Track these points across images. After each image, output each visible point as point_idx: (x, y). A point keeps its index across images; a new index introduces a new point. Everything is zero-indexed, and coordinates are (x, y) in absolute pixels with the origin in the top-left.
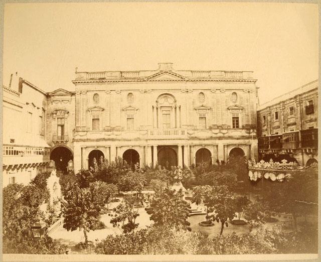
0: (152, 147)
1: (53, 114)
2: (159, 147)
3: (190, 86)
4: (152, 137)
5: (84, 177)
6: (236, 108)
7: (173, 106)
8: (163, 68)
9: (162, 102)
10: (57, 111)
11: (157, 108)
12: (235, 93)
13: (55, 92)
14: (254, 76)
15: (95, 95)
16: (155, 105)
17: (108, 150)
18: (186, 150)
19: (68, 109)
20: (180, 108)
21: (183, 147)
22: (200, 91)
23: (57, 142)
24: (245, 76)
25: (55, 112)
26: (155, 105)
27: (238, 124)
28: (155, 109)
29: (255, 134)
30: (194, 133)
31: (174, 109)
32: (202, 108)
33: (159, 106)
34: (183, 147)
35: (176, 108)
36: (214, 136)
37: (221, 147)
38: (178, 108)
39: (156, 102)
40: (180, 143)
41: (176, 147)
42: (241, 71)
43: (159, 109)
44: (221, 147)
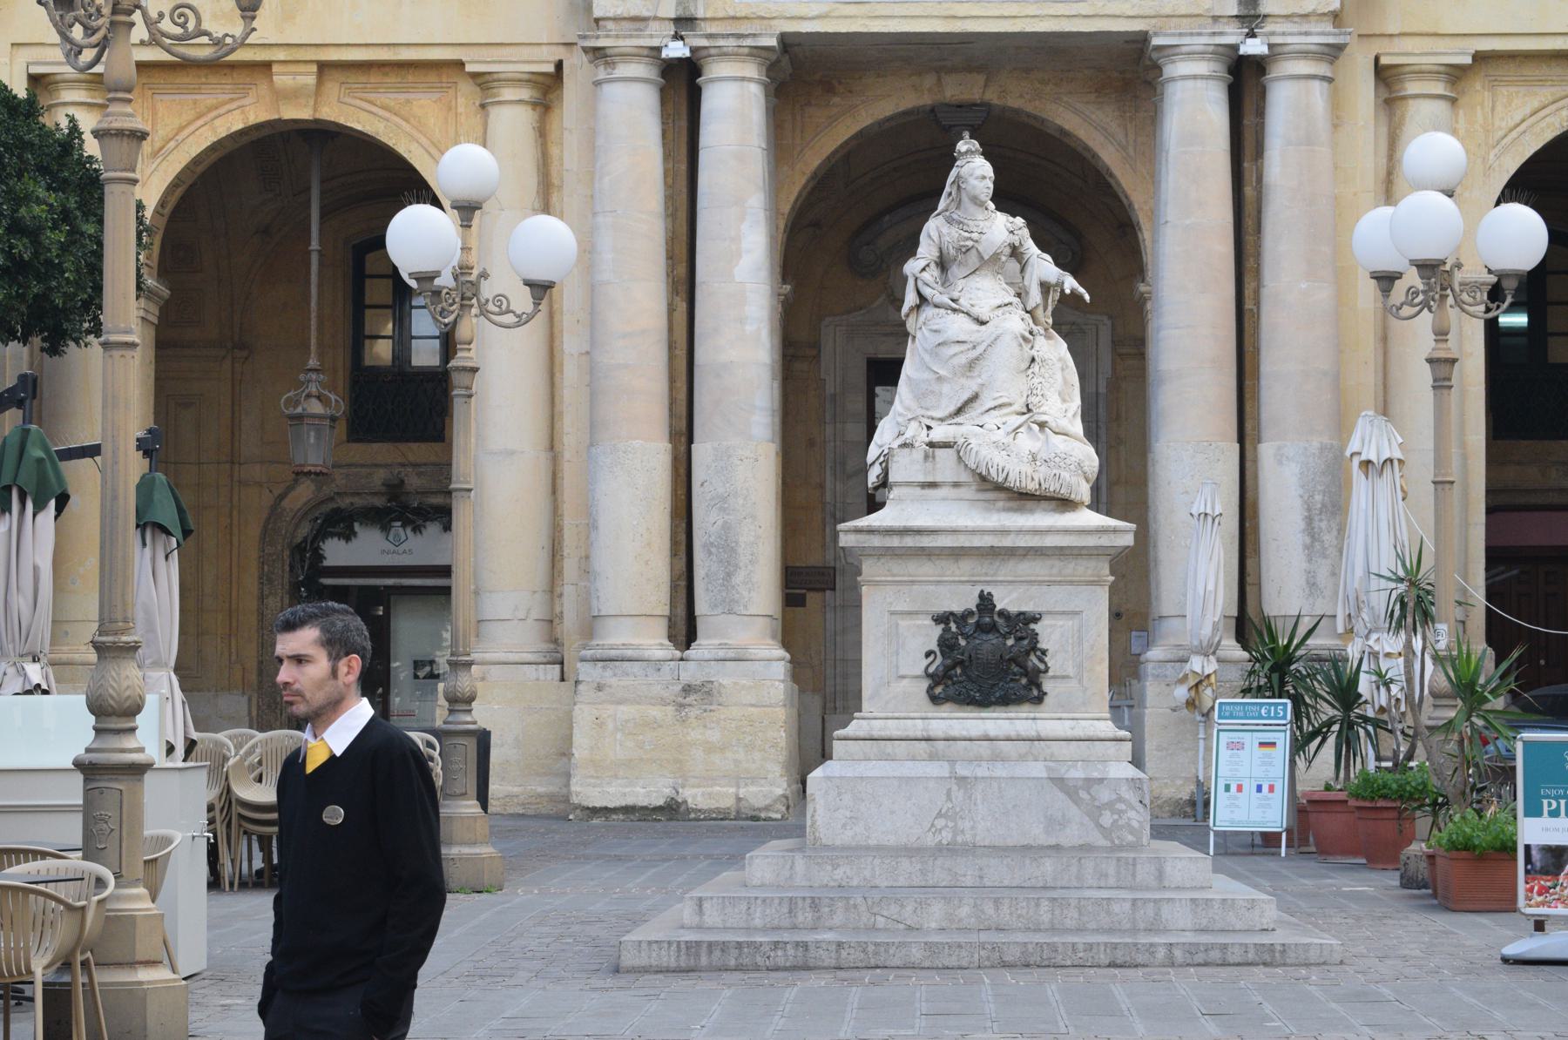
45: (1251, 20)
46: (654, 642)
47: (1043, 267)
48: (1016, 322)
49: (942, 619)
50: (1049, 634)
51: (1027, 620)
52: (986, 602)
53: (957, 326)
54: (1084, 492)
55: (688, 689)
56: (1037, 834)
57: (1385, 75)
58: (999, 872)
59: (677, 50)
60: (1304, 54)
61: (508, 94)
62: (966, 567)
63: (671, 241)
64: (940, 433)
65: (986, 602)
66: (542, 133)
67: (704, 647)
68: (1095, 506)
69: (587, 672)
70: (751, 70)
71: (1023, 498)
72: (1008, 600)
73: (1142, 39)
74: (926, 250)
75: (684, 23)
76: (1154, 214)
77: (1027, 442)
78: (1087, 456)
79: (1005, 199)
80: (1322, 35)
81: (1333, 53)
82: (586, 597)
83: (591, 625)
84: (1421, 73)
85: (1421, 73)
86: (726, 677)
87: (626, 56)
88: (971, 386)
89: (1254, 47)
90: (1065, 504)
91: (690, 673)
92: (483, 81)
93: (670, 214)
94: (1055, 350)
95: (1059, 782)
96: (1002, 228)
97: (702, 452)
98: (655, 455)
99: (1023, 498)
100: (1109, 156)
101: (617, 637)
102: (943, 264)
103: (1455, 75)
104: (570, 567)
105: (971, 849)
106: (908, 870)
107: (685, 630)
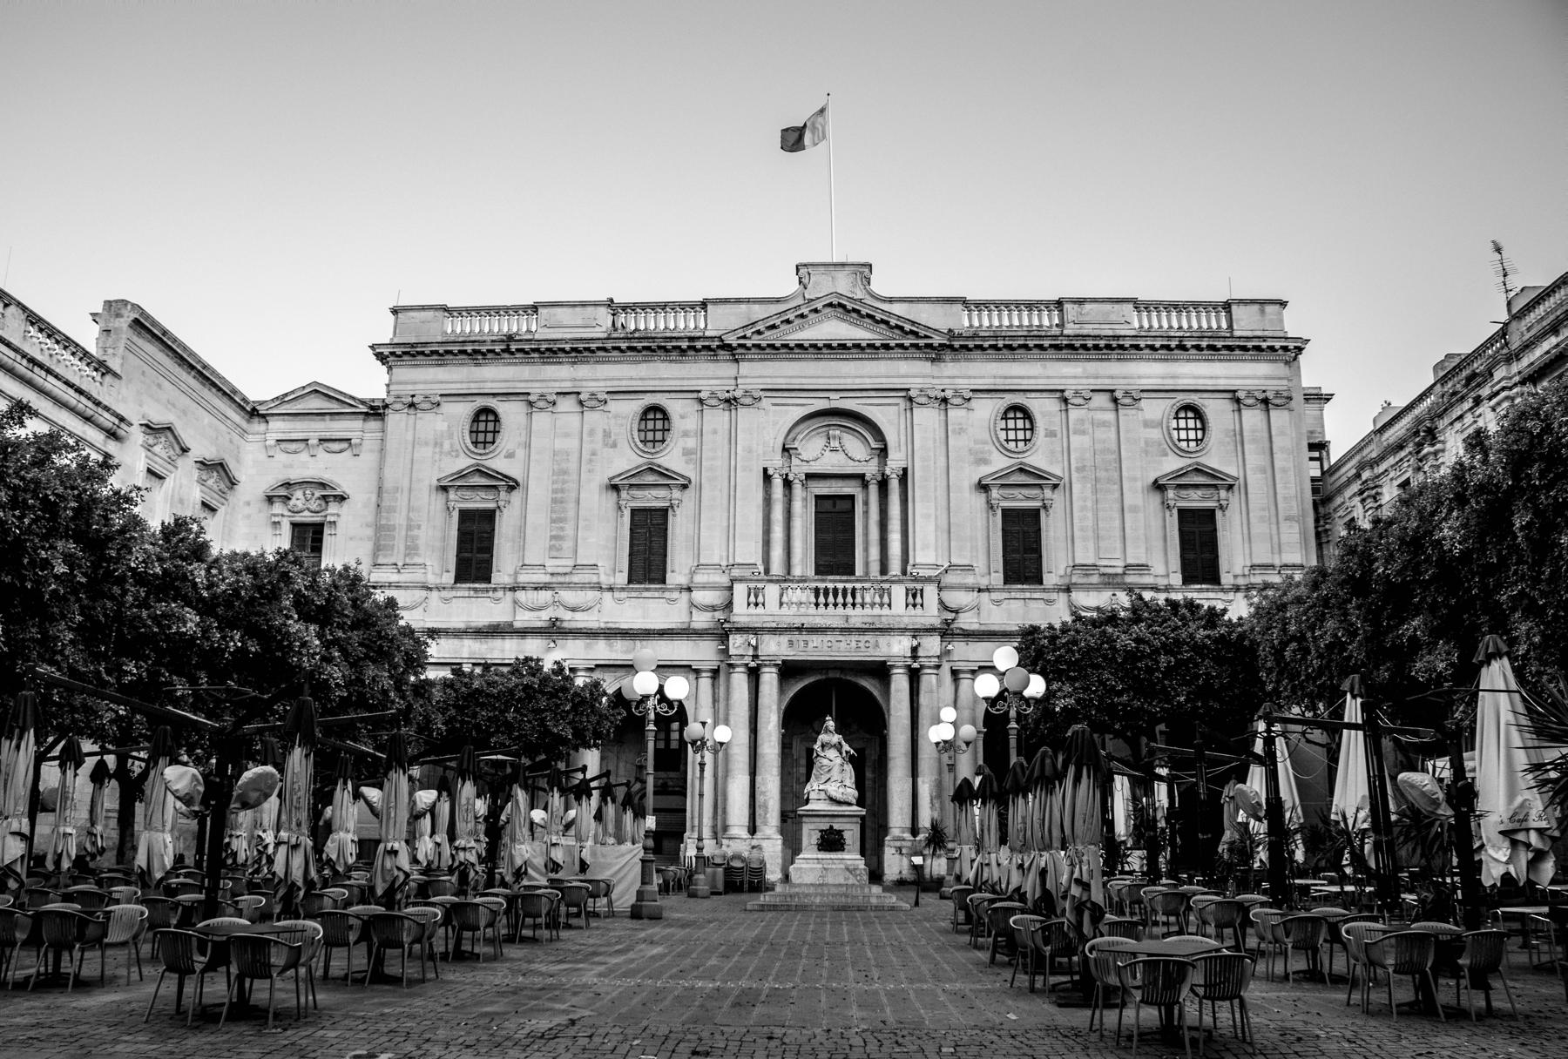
2: (789, 671)
6: (1200, 480)
7: (871, 469)
8: (822, 287)
9: (817, 453)
10: (287, 485)
11: (788, 484)
14: (1293, 324)
15: (476, 418)
16: (776, 462)
19: (344, 484)
20: (904, 477)
24: (1246, 323)
25: (283, 492)
26: (776, 462)
28: (778, 483)
31: (873, 490)
33: (798, 469)
35: (883, 484)
38: (894, 485)
39: (785, 450)
40: (896, 648)
43: (798, 489)
45: (915, 657)
46: (744, 833)
47: (846, 747)
48: (839, 761)
49: (821, 831)
50: (846, 835)
51: (840, 832)
52: (831, 827)
53: (825, 762)
54: (854, 801)
55: (753, 847)
56: (842, 881)
57: (955, 673)
58: (834, 890)
59: (753, 664)
60: (930, 667)
61: (704, 674)
62: (827, 819)
63: (750, 717)
64: (821, 787)
65: (831, 827)
66: (713, 685)
67: (758, 835)
68: (858, 805)
69: (725, 842)
70: (774, 670)
71: (839, 803)
72: (836, 827)
73: (885, 662)
74: (819, 743)
75: (755, 657)
76: (889, 711)
77: (841, 790)
78: (856, 793)
79: (838, 731)
80: (935, 661)
81: (938, 667)
82: (724, 820)
83: (725, 828)
84: (964, 672)
85: (964, 672)
86: (764, 844)
87: (738, 666)
88: (828, 776)
89: (916, 665)
90: (850, 804)
91: (754, 842)
92: (697, 672)
93: (750, 710)
94: (849, 768)
95: (847, 869)
96: (836, 738)
97: (759, 779)
98: (746, 779)
99: (839, 803)
100: (876, 693)
101: (734, 831)
102: (823, 746)
103: (973, 672)
104: (720, 811)
105: (827, 885)
106: (812, 890)
107: (753, 829)
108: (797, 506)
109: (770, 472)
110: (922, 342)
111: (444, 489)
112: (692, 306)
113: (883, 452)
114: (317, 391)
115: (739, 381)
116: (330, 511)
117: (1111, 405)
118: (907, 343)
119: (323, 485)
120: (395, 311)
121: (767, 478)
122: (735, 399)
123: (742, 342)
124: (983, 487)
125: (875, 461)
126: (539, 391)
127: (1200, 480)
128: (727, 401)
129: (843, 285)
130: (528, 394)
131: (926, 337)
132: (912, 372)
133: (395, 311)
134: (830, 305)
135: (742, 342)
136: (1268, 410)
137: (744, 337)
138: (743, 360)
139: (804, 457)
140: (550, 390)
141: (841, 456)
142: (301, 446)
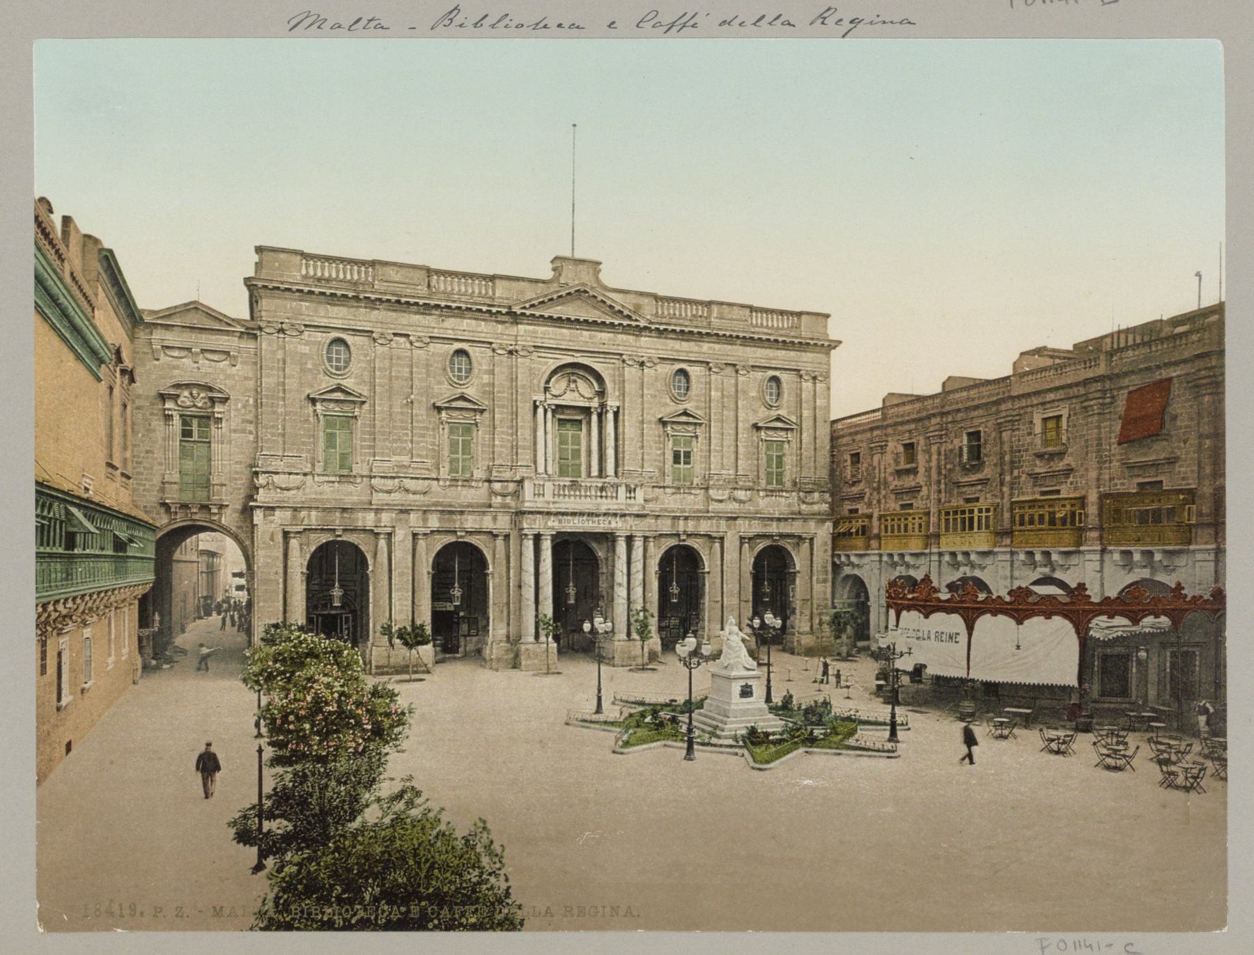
0: (537, 538)
1: (163, 397)
3: (648, 346)
4: (540, 504)
5: (769, 618)
6: (779, 425)
8: (572, 278)
10: (178, 386)
12: (683, 372)
13: (171, 313)
17: (717, 545)
18: (638, 544)
21: (630, 540)
22: (771, 373)
23: (185, 506)
24: (806, 330)
25: (172, 392)
27: (590, 472)
29: (825, 507)
30: (656, 499)
31: (594, 418)
32: (684, 419)
34: (630, 540)
36: (714, 506)
37: (731, 543)
41: (608, 538)
42: (798, 310)
44: (731, 543)
92: (496, 536)
108: (549, 424)
109: (538, 403)
110: (634, 324)
111: (313, 401)
112: (485, 277)
113: (602, 394)
114: (194, 307)
115: (519, 338)
116: (216, 409)
117: (734, 374)
118: (625, 323)
119: (210, 389)
120: (259, 250)
121: (536, 407)
122: (517, 351)
123: (524, 311)
124: (663, 423)
125: (596, 399)
126: (379, 330)
127: (779, 425)
128: (511, 352)
129: (584, 278)
130: (372, 332)
131: (636, 320)
132: (624, 342)
133: (259, 250)
134: (577, 291)
135: (524, 311)
136: (815, 383)
137: (524, 308)
138: (521, 324)
139: (554, 392)
140: (389, 331)
141: (576, 394)
142: (183, 353)
